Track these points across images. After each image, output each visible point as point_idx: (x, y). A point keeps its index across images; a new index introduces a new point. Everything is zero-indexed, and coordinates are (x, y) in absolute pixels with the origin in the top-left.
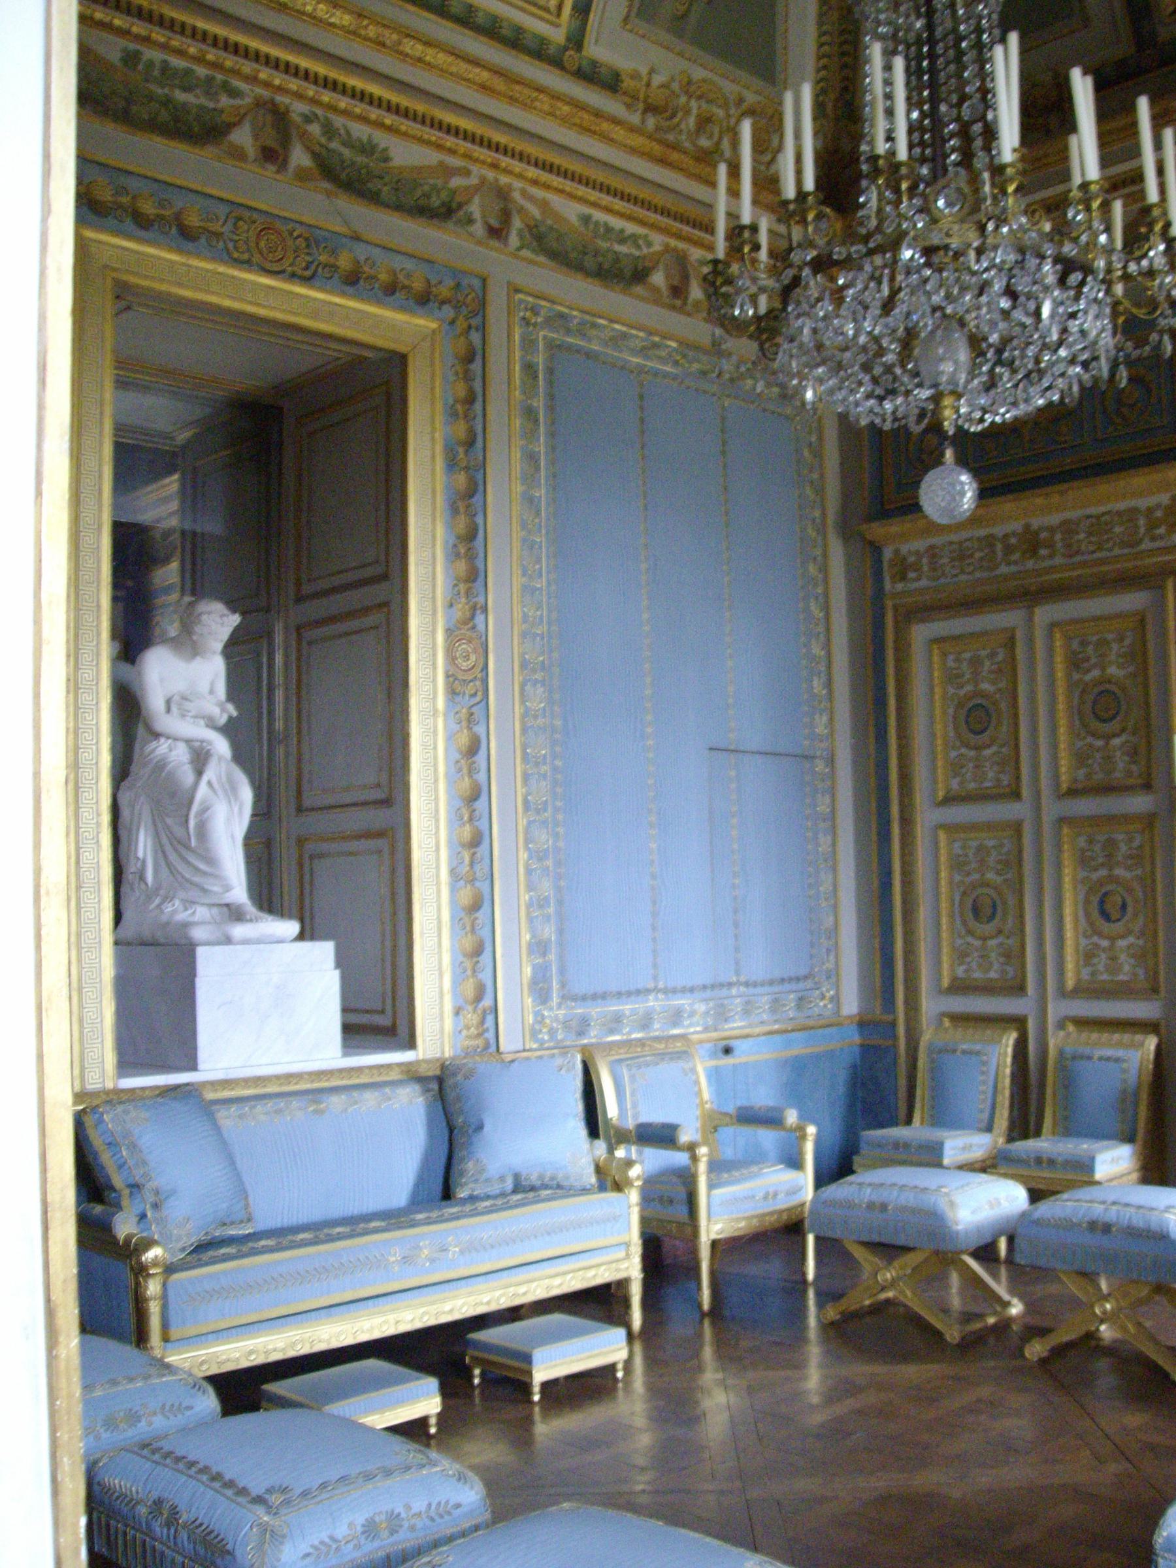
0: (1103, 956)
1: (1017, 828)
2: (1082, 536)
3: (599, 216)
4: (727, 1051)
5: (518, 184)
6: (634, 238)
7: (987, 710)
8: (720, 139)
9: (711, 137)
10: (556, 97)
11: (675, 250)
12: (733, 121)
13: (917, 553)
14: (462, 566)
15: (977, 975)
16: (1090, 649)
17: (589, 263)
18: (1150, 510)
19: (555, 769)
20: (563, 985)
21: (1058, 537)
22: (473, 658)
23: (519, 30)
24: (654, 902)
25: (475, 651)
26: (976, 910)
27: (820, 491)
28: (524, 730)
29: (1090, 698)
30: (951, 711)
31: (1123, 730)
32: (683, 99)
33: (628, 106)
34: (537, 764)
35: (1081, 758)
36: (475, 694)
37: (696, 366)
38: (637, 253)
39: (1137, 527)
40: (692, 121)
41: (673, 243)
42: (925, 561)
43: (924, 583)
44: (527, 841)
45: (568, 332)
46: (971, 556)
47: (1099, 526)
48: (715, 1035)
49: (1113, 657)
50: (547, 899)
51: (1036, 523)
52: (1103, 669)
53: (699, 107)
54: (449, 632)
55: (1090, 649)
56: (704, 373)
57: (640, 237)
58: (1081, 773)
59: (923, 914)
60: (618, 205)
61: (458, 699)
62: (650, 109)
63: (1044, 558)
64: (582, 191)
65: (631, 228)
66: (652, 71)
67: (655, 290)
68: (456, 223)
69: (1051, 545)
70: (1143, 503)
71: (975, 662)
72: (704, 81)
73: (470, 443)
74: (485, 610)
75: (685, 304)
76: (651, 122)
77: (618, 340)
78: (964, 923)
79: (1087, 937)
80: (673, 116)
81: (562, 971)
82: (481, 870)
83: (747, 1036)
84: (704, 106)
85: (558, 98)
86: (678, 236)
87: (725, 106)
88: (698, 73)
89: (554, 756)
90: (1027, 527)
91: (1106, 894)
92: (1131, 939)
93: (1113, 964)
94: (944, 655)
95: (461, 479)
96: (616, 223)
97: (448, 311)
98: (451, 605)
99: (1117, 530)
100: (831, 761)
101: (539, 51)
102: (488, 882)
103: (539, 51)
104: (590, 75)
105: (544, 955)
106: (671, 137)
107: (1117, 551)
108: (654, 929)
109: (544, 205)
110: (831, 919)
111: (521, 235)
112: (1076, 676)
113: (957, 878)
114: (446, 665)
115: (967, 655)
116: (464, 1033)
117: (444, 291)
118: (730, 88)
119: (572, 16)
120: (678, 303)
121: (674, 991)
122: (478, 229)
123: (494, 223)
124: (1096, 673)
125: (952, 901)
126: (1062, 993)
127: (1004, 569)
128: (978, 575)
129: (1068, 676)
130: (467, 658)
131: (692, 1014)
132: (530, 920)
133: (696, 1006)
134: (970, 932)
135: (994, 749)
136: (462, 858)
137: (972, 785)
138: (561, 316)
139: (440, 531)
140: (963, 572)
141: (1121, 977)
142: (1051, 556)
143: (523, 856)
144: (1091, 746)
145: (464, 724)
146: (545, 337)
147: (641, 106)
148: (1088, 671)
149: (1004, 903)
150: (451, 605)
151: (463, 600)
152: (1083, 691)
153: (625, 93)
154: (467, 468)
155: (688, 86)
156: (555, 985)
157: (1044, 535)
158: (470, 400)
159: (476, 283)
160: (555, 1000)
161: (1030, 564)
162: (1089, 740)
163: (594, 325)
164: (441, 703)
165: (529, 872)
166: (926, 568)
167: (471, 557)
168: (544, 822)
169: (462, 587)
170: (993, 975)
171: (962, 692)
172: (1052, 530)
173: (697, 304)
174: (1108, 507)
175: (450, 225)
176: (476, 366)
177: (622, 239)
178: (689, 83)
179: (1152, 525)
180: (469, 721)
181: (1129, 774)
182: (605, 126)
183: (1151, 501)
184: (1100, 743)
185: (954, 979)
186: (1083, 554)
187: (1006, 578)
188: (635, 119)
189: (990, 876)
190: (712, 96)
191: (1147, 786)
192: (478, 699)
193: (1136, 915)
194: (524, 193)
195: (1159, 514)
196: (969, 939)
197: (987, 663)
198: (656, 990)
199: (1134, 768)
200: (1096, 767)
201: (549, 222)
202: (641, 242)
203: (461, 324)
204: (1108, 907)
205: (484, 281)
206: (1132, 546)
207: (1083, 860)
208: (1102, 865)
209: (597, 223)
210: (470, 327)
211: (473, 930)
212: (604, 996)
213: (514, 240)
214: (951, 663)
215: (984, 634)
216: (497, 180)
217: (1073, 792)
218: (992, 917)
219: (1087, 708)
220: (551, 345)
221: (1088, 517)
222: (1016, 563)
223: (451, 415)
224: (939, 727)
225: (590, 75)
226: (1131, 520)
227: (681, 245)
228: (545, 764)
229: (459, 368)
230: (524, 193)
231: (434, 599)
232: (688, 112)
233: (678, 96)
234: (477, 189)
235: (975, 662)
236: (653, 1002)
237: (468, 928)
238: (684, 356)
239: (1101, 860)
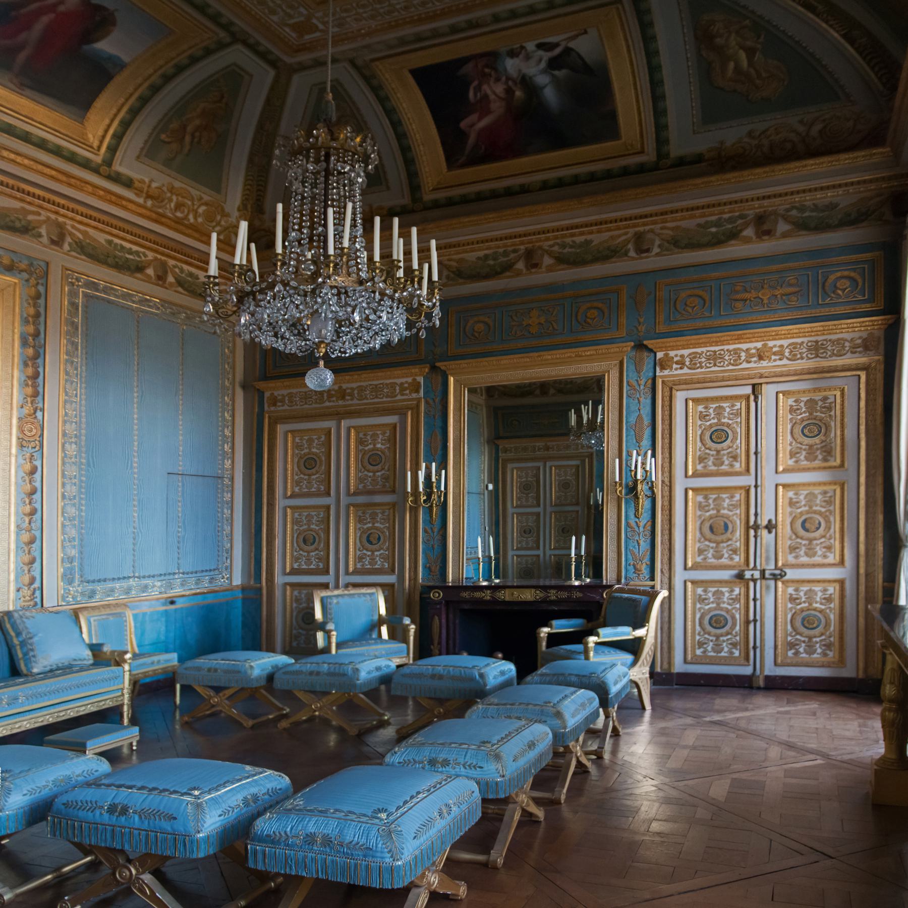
0: (368, 558)
1: (328, 508)
2: (368, 392)
3: (116, 241)
4: (172, 603)
5: (68, 222)
6: (137, 253)
7: (315, 461)
8: (188, 214)
9: (183, 212)
10: (95, 186)
11: (160, 259)
12: (196, 207)
13: (283, 395)
14: (29, 390)
15: (304, 567)
16: (369, 437)
17: (110, 260)
18: (402, 384)
19: (81, 481)
20: (81, 577)
21: (356, 392)
22: (34, 431)
23: (74, 154)
24: (134, 539)
25: (36, 428)
26: (305, 541)
27: (233, 368)
28: (64, 463)
29: (367, 457)
30: (296, 460)
31: (383, 469)
32: (169, 195)
33: (137, 195)
34: (71, 479)
35: (361, 480)
36: (35, 448)
37: (168, 311)
38: (139, 259)
39: (395, 390)
40: (173, 205)
41: (159, 256)
42: (287, 398)
43: (286, 407)
44: (63, 513)
45: (97, 290)
46: (311, 398)
47: (376, 390)
48: (165, 596)
49: (380, 441)
50: (74, 538)
51: (344, 386)
52: (374, 445)
53: (177, 199)
54: (20, 419)
55: (369, 437)
56: (174, 314)
57: (141, 252)
58: (361, 486)
59: (278, 542)
60: (129, 237)
61: (24, 449)
62: (149, 196)
63: (348, 400)
64: (108, 229)
65: (135, 248)
66: (152, 181)
67: (149, 276)
68: (30, 236)
69: (351, 395)
70: (398, 381)
71: (310, 441)
72: (181, 188)
73: (36, 335)
74: (43, 410)
75: (165, 282)
76: (149, 203)
77: (125, 296)
78: (298, 545)
79: (359, 550)
80: (162, 201)
81: (81, 570)
82: (36, 525)
83: (183, 596)
84: (180, 199)
85: (97, 188)
86: (162, 254)
87: (192, 200)
88: (177, 184)
89: (82, 475)
90: (340, 387)
91: (371, 533)
92: (382, 551)
93: (373, 561)
94: (294, 438)
95: (30, 351)
96: (127, 245)
97: (25, 276)
98: (22, 407)
99: (385, 390)
100: (232, 479)
101: (86, 164)
102: (39, 531)
103: (86, 164)
104: (116, 178)
105: (71, 563)
106: (160, 210)
107: (385, 399)
108: (134, 550)
109: (85, 234)
110: (229, 545)
111: (70, 244)
112: (361, 447)
113: (296, 527)
114: (17, 434)
115: (306, 438)
116: (22, 599)
117: (23, 266)
118: (195, 192)
119: (106, 152)
120: (160, 283)
121: (144, 577)
122: (45, 240)
123: (55, 238)
124: (371, 446)
125: (293, 537)
126: (347, 573)
127: (327, 404)
128: (314, 406)
129: (357, 447)
130: (31, 431)
131: (154, 586)
132: (63, 547)
133: (156, 583)
134: (301, 549)
135: (317, 476)
136: (24, 521)
137: (306, 490)
138: (94, 283)
139: (16, 373)
140: (306, 403)
141: (377, 566)
142: (352, 400)
143: (60, 519)
144: (367, 475)
145: (28, 460)
146: (83, 292)
147: (144, 195)
148: (368, 445)
149: (320, 537)
150: (22, 407)
151: (30, 405)
152: (364, 454)
153: (136, 189)
154: (34, 347)
155: (172, 190)
156: (77, 576)
157: (348, 391)
158: (37, 315)
159: (42, 264)
160: (77, 583)
161: (341, 402)
162: (366, 473)
163: (112, 289)
164: (14, 451)
165: (63, 526)
166: (287, 402)
167: (35, 386)
168: (74, 505)
169: (29, 399)
170: (312, 567)
171: (302, 452)
172: (353, 389)
173: (171, 284)
174: (382, 382)
175: (27, 237)
176: (41, 301)
177: (130, 252)
178: (173, 188)
179: (402, 390)
180: (31, 459)
181: (384, 486)
182: (124, 203)
183: (403, 380)
184: (371, 474)
185: (292, 569)
186: (367, 399)
187: (328, 407)
188: (141, 201)
189: (313, 527)
190: (185, 195)
191: (393, 491)
192: (37, 449)
193: (385, 542)
194: (73, 227)
195: (406, 385)
196: (301, 552)
197: (316, 441)
198: (134, 577)
199: (387, 484)
200: (368, 484)
201: (88, 241)
202: (141, 255)
203: (33, 281)
204: (371, 539)
205: (47, 264)
206: (392, 397)
207: (360, 520)
208: (369, 522)
209: (116, 244)
210: (38, 284)
211: (29, 552)
212: (105, 580)
213: (66, 247)
214: (297, 440)
215: (315, 429)
216: (57, 219)
217: (355, 494)
218: (312, 544)
219: (366, 460)
220: (85, 295)
221: (371, 385)
222: (333, 401)
223: (25, 322)
224: (289, 466)
225: (116, 178)
226: (392, 387)
227: (163, 258)
228: (75, 478)
229: (31, 301)
230: (73, 227)
231: (11, 404)
232: (170, 200)
233: (166, 193)
234: (45, 222)
235: (310, 441)
236: (132, 582)
237: (27, 552)
238: (162, 306)
239: (369, 520)
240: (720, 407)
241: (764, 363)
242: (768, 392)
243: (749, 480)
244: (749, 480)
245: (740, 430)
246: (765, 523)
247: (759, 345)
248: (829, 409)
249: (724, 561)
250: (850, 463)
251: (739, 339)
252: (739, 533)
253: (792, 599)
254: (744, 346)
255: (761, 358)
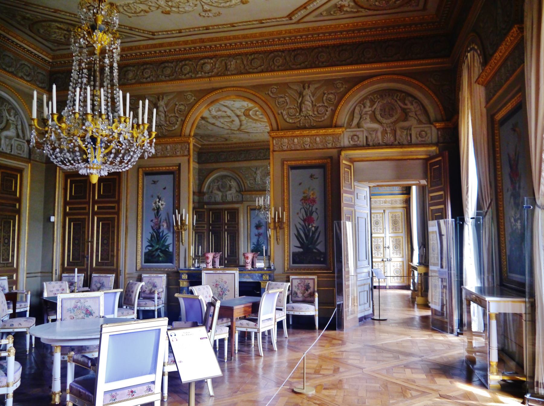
240: (377, 215)
241: (386, 204)
242: (387, 212)
243: (383, 235)
244: (383, 235)
245: (381, 222)
246: (387, 246)
247: (384, 199)
248: (399, 217)
249: (379, 256)
250: (403, 232)
251: (381, 198)
252: (382, 249)
253: (394, 266)
254: (381, 199)
255: (385, 203)
